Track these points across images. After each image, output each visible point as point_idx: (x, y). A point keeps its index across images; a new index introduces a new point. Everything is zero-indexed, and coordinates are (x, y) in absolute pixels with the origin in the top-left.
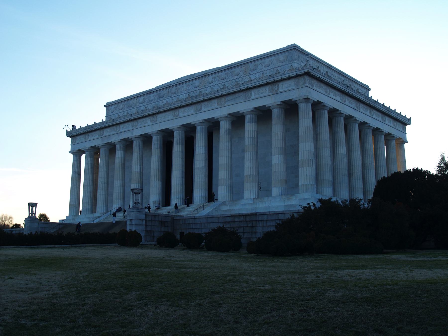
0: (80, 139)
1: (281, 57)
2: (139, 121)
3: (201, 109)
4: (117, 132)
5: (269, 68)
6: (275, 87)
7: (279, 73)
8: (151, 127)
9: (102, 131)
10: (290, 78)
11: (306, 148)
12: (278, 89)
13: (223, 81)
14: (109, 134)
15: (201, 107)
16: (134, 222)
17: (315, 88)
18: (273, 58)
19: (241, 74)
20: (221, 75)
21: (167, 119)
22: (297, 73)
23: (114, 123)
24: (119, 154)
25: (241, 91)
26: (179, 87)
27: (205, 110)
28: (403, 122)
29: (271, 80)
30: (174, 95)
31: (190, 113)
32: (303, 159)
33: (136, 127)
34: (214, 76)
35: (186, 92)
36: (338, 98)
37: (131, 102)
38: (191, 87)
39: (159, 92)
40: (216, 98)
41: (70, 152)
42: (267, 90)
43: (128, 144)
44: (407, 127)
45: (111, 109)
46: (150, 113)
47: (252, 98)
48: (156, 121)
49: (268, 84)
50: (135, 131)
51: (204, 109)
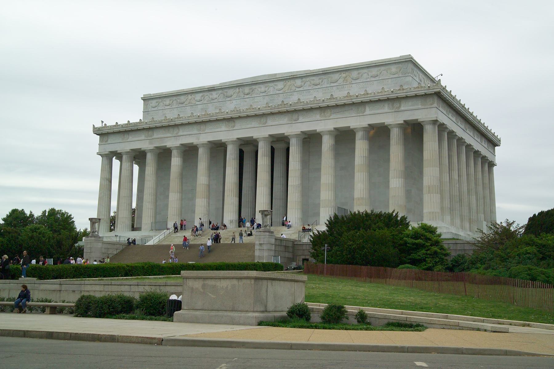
0: (111, 139)
1: (394, 69)
3: (298, 119)
4: (174, 135)
5: (377, 78)
6: (396, 105)
7: (403, 89)
8: (229, 135)
9: (150, 132)
10: (416, 96)
11: (431, 174)
12: (400, 107)
13: (317, 87)
14: (162, 136)
15: (298, 116)
16: (265, 247)
17: (440, 109)
18: (382, 68)
19: (341, 81)
20: (313, 80)
21: (249, 126)
22: (425, 91)
23: (172, 123)
24: (176, 161)
25: (353, 104)
26: (254, 87)
27: (303, 120)
28: (493, 143)
30: (248, 96)
31: (281, 122)
32: (429, 184)
35: (264, 94)
36: (454, 119)
37: (183, 98)
38: (271, 89)
40: (320, 108)
41: (98, 154)
42: (386, 108)
43: (189, 152)
44: (496, 148)
46: (226, 116)
47: (366, 113)
48: (234, 127)
49: (388, 100)
50: (202, 137)
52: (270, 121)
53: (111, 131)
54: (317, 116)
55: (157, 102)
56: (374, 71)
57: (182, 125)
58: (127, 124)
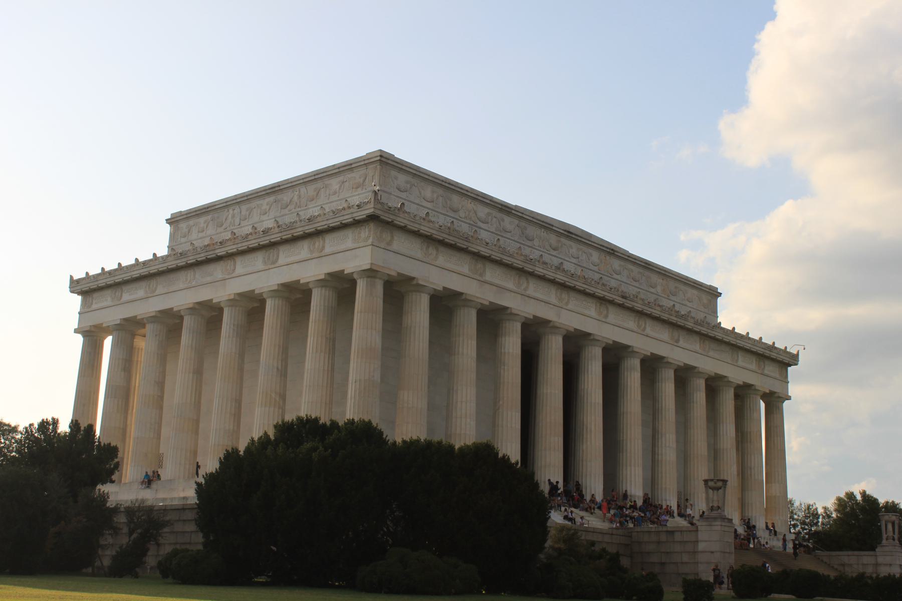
2: (572, 294)
3: (677, 341)
18: (695, 292)
19: (659, 289)
23: (529, 268)
26: (563, 240)
29: (767, 353)
30: (554, 253)
33: (567, 304)
34: (622, 263)
35: (574, 261)
37: (455, 198)
39: (523, 224)
45: (396, 178)
48: (606, 316)
51: (682, 343)
52: (651, 328)
53: (414, 227)
54: (695, 344)
55: (407, 182)
56: (691, 293)
57: (542, 278)
58: (449, 228)
